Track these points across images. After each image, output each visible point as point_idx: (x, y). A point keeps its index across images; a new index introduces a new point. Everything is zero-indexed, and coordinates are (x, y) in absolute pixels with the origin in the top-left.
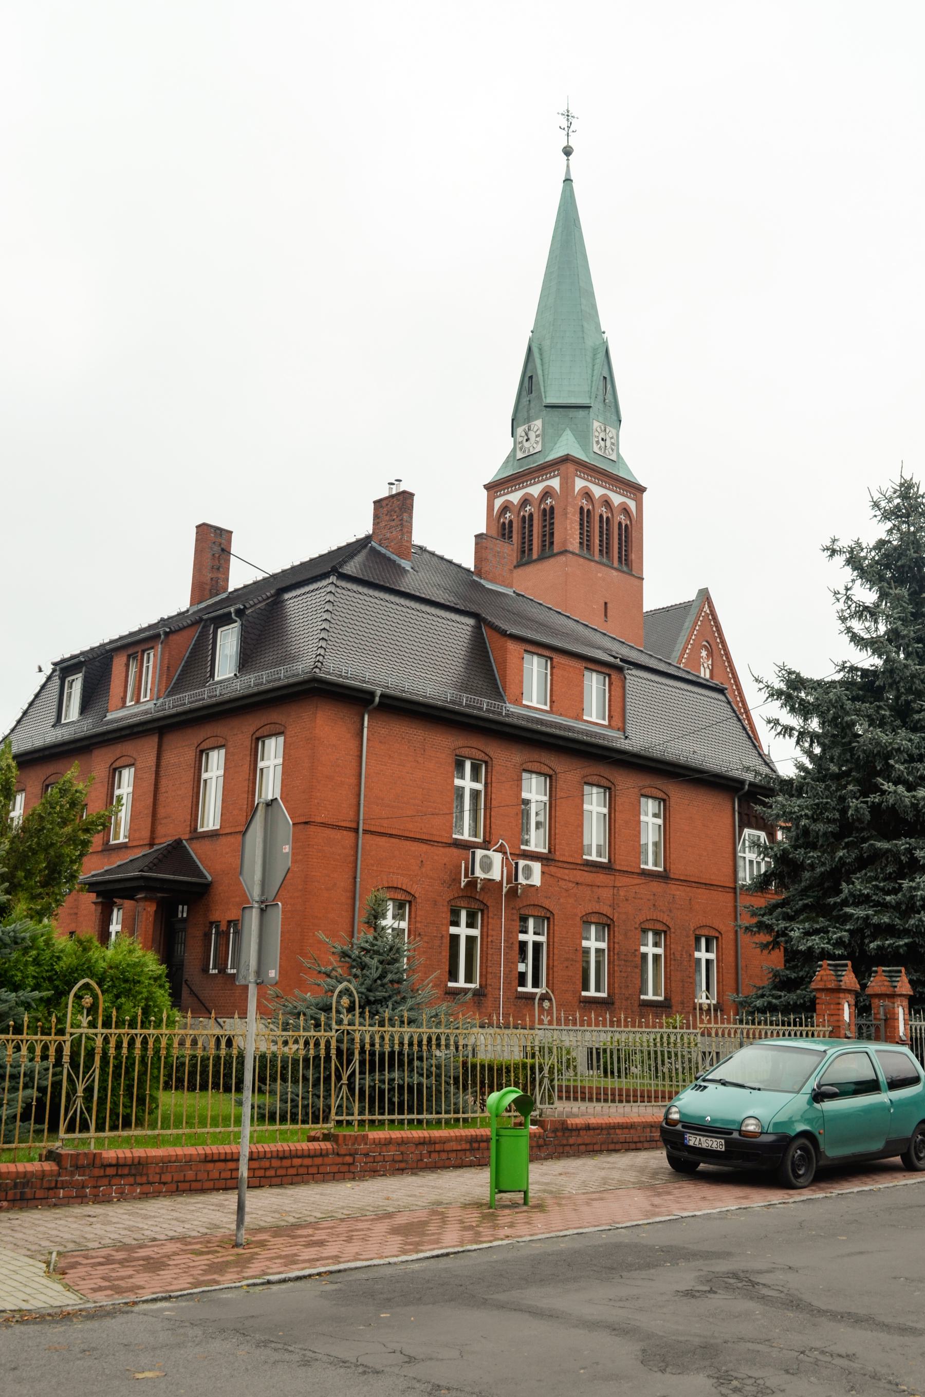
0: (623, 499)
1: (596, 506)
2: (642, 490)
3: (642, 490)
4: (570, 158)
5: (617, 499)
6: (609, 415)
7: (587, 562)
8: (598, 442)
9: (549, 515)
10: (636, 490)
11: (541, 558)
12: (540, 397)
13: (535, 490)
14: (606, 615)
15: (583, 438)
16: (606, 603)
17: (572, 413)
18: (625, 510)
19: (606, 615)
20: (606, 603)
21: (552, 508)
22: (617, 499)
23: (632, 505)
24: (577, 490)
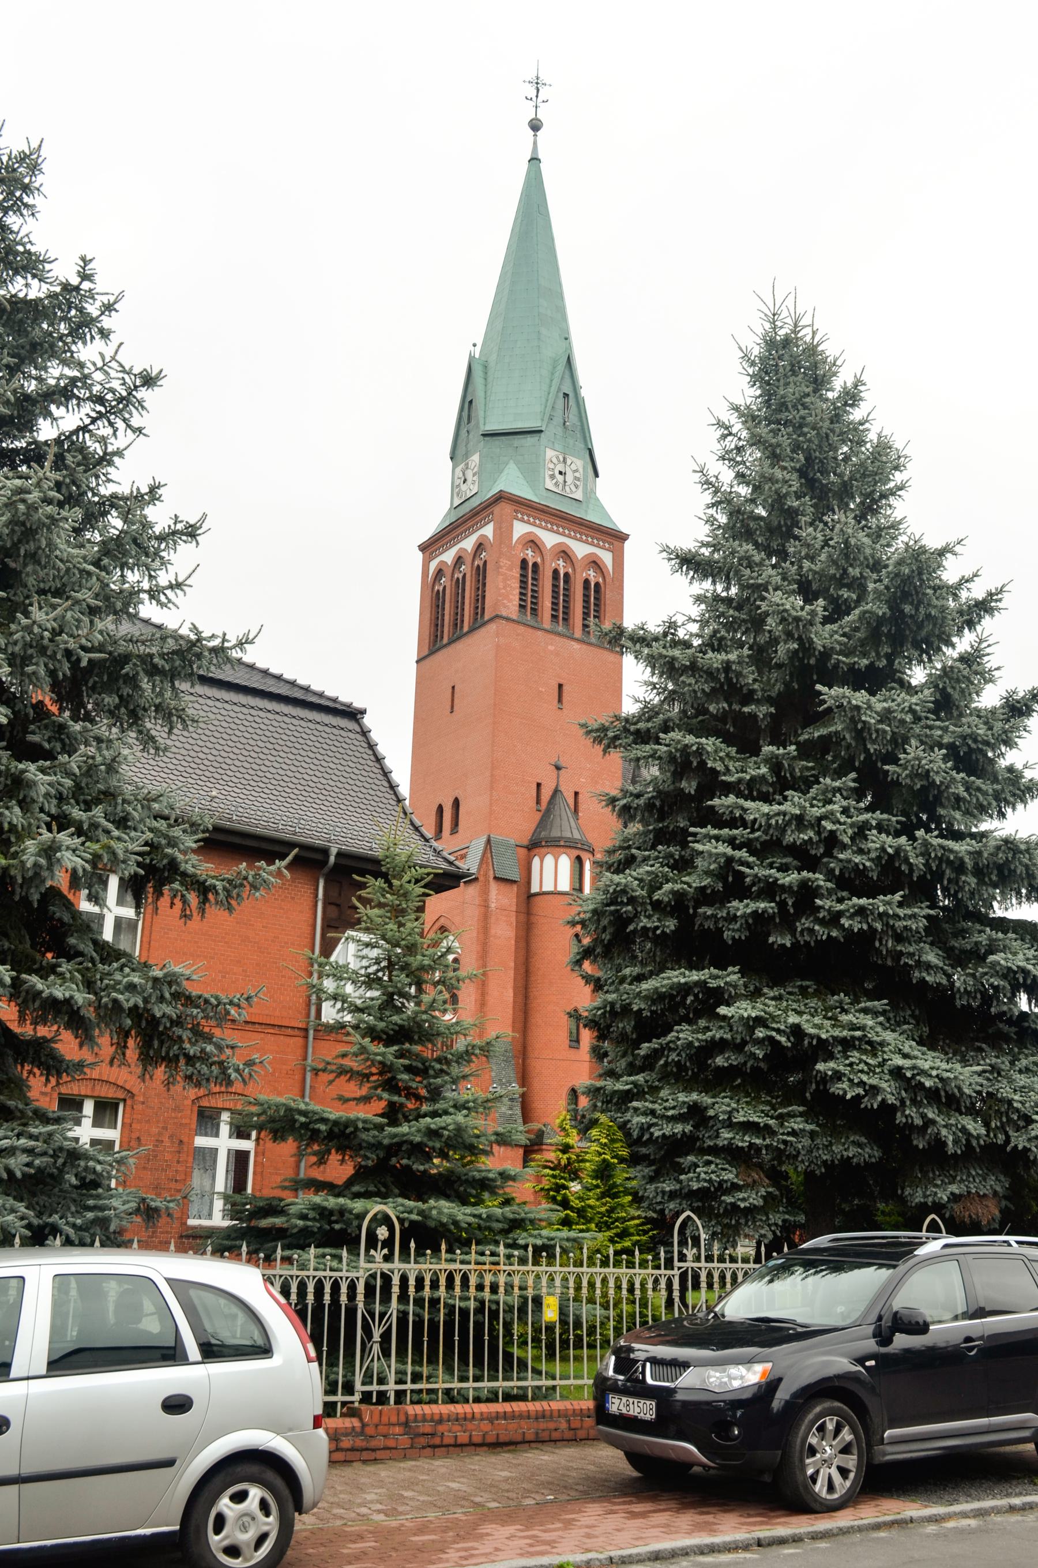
0: (590, 549)
1: (548, 558)
2: (623, 538)
3: (623, 538)
5: (581, 550)
6: (571, 441)
7: (530, 630)
9: (481, 573)
10: (615, 538)
11: (472, 630)
12: (477, 426)
13: (468, 544)
14: (560, 700)
15: (532, 472)
16: (560, 686)
17: (517, 441)
18: (595, 563)
19: (560, 700)
20: (560, 686)
22: (581, 550)
23: (607, 558)
24: (515, 539)
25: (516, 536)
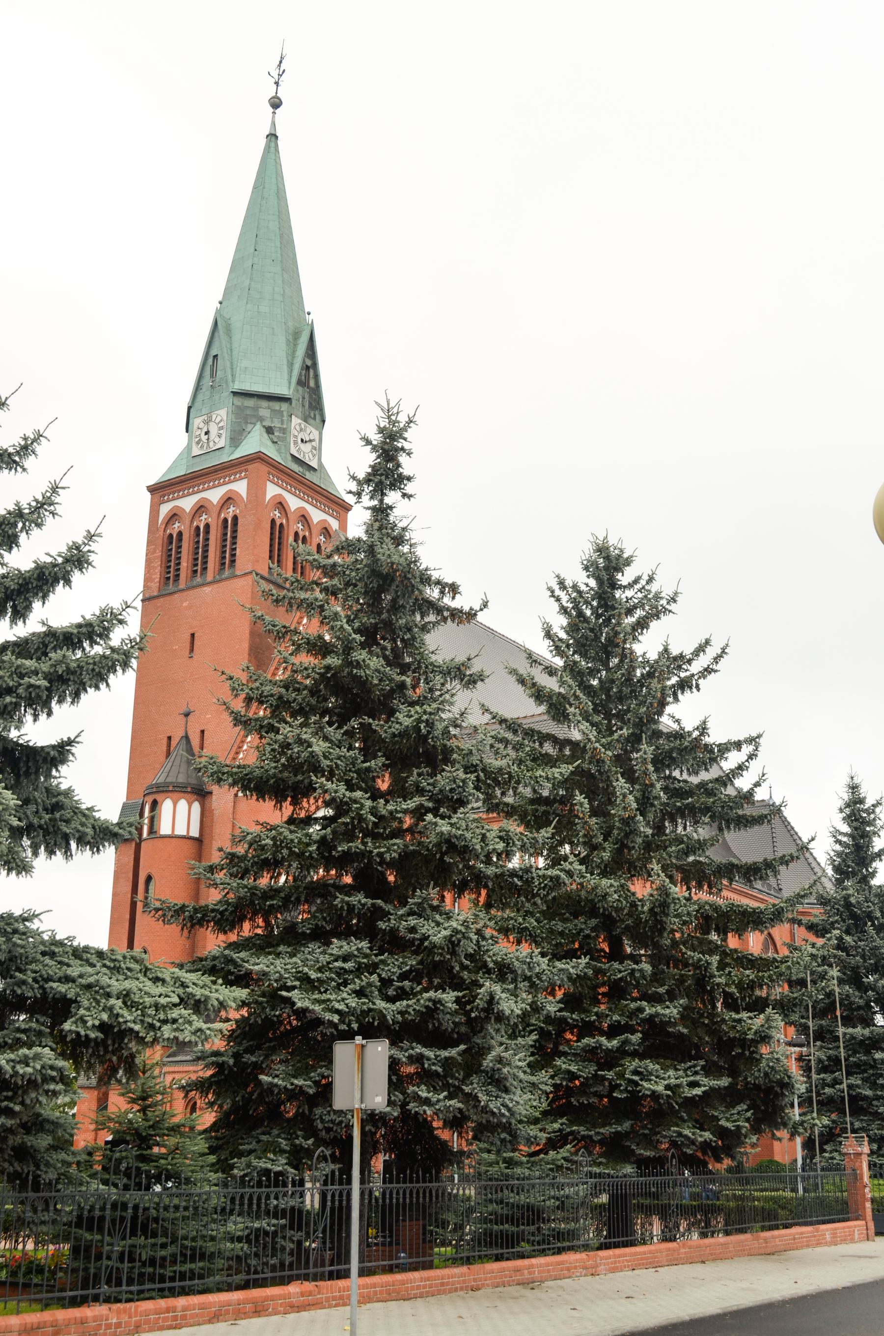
4: (277, 111)
8: (296, 443)
21: (235, 518)
25: (268, 497)
